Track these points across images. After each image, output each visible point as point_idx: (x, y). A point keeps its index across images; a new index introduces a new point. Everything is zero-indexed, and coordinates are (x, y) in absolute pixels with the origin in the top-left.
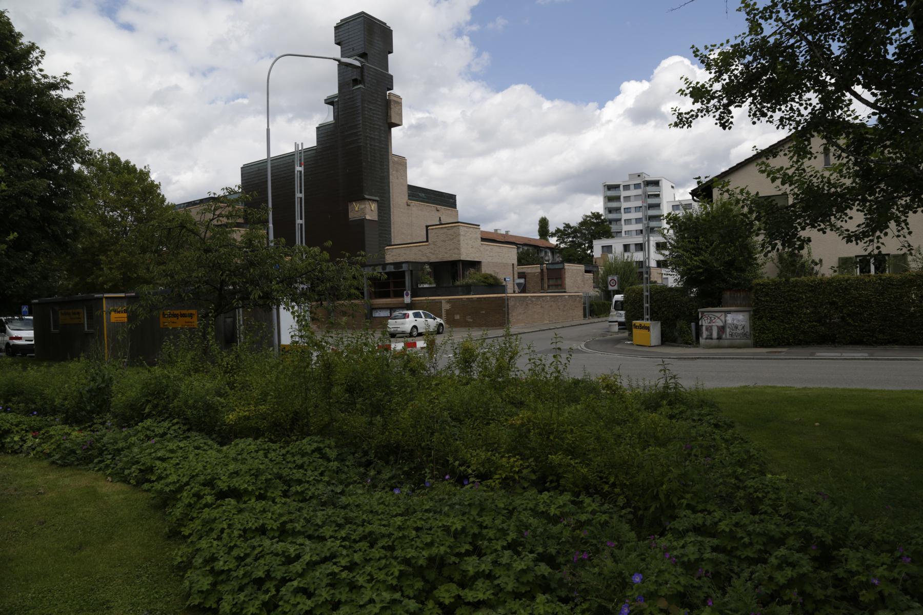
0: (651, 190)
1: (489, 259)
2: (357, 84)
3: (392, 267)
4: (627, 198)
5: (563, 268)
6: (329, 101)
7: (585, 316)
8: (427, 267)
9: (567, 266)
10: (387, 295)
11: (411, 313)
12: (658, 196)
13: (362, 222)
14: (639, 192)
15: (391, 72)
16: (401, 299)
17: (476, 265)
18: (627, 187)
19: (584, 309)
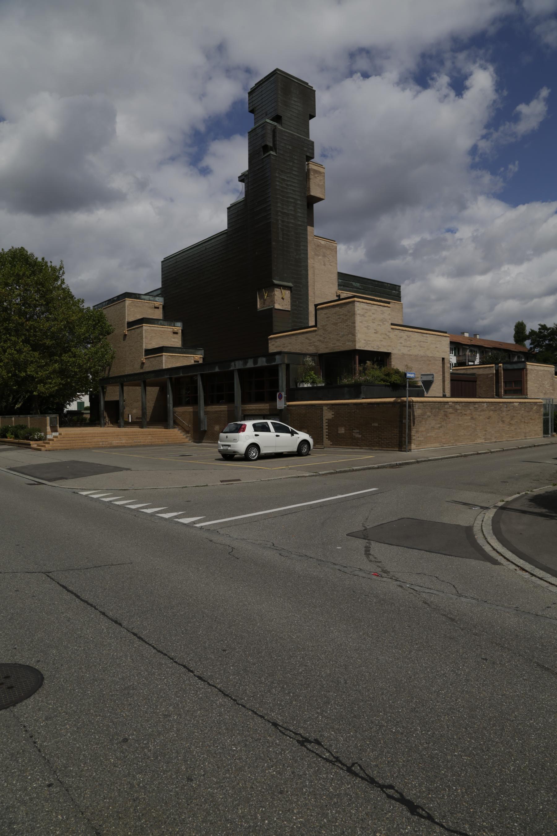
1: (405, 351)
2: (268, 152)
5: (524, 369)
6: (242, 179)
7: (546, 432)
8: (308, 359)
9: (530, 366)
10: (259, 399)
11: (249, 424)
13: (270, 312)
15: (312, 138)
17: (382, 358)
19: (546, 422)
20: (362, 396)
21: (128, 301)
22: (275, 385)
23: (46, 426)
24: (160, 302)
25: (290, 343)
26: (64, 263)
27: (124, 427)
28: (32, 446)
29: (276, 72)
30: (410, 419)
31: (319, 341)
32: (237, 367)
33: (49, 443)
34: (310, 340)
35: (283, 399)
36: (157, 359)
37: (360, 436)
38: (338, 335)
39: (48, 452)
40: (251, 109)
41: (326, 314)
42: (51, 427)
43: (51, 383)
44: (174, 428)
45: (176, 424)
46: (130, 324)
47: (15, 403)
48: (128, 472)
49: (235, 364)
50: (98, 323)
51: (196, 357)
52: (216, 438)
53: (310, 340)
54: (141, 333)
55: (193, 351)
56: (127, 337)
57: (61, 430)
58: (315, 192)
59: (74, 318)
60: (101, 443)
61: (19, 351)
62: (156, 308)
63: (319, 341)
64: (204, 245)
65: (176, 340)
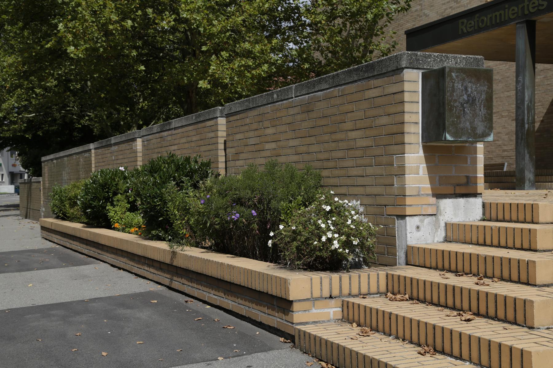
23: (396, 138)
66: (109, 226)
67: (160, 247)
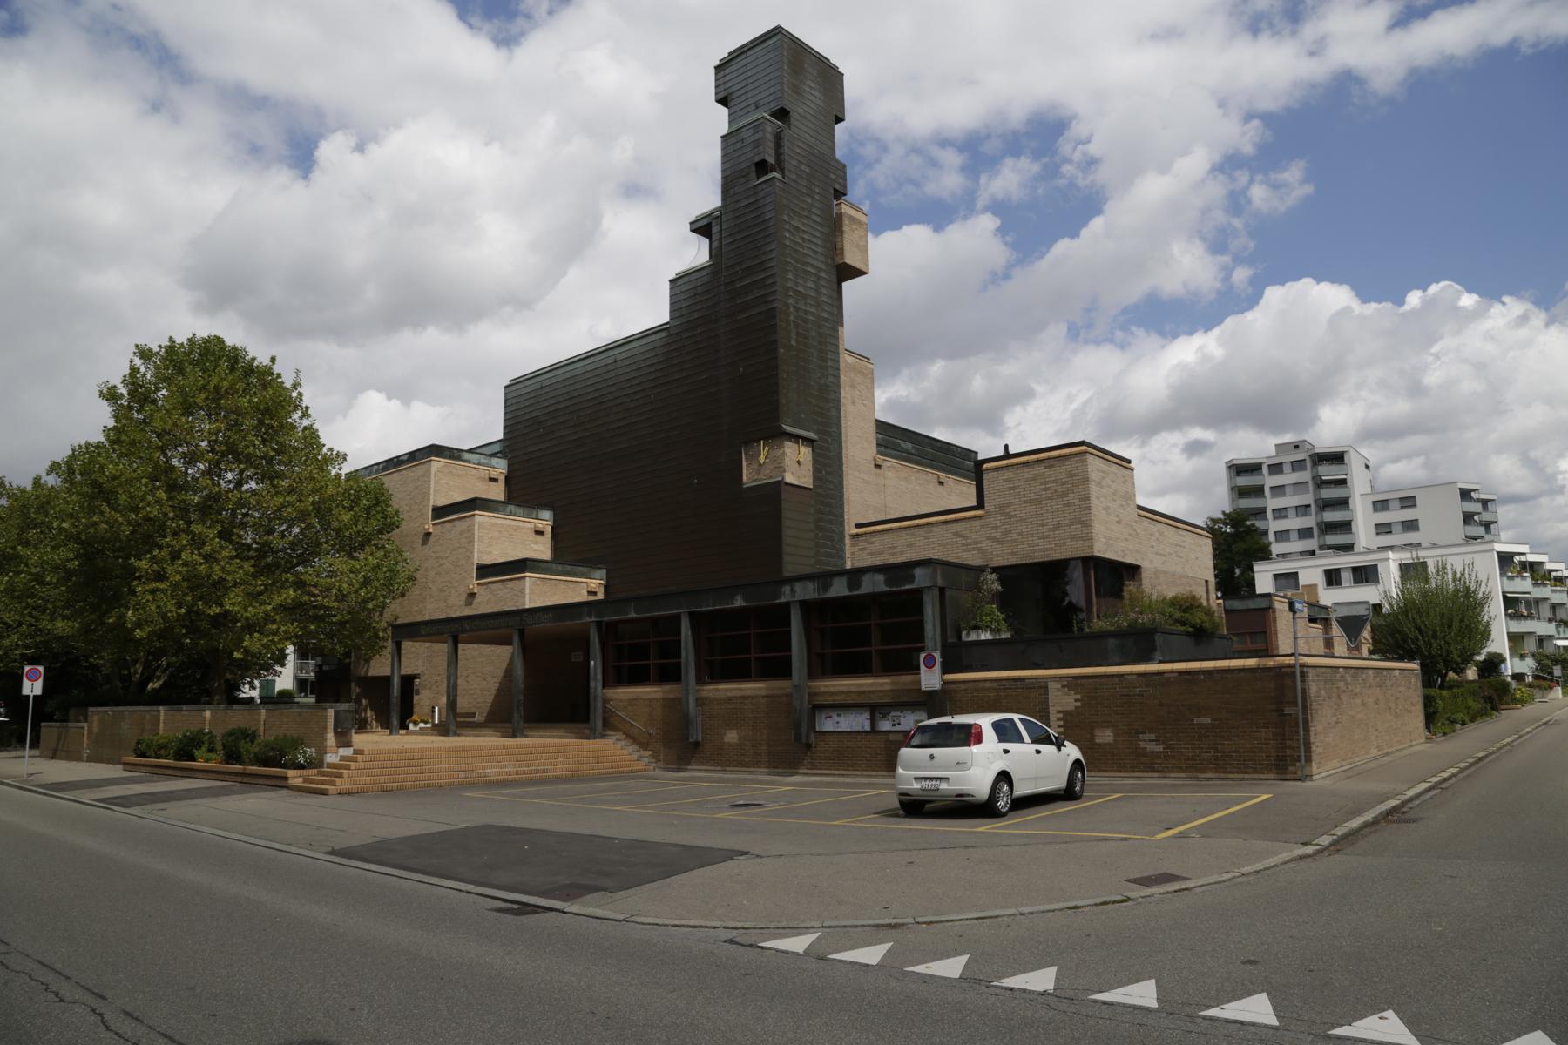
0: (1328, 472)
3: (880, 578)
4: (1278, 490)
6: (702, 227)
11: (985, 721)
12: (1343, 482)
13: (774, 492)
14: (1305, 476)
16: (907, 679)
18: (1276, 469)
20: (1158, 656)
21: (437, 464)
22: (916, 633)
23: (325, 729)
24: (500, 467)
25: (910, 546)
26: (301, 375)
27: (456, 734)
28: (291, 782)
29: (777, 31)
30: (1305, 707)
31: (994, 539)
32: (800, 596)
33: (340, 776)
34: (962, 536)
35: (938, 667)
36: (510, 584)
37: (1160, 748)
38: (1043, 525)
39: (346, 798)
40: (721, 95)
41: (1008, 480)
42: (336, 733)
43: (275, 633)
44: (603, 736)
45: (609, 724)
46: (440, 512)
47: (149, 679)
48: (1132, 876)
49: (792, 590)
50: (367, 507)
51: (584, 587)
52: (890, 764)
53: (962, 536)
54: (470, 530)
55: (585, 570)
56: (432, 539)
57: (358, 739)
58: (851, 258)
59: (331, 490)
60: (462, 774)
61: (208, 558)
62: (491, 479)
63: (994, 539)
64: (611, 353)
65: (540, 547)
66: (194, 760)
67: (237, 768)
